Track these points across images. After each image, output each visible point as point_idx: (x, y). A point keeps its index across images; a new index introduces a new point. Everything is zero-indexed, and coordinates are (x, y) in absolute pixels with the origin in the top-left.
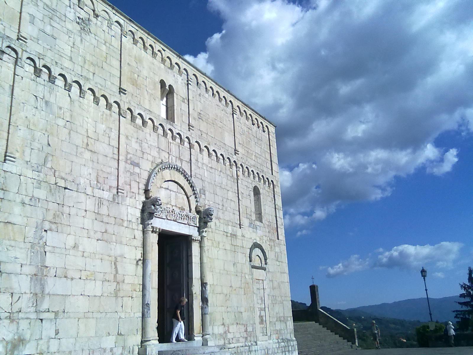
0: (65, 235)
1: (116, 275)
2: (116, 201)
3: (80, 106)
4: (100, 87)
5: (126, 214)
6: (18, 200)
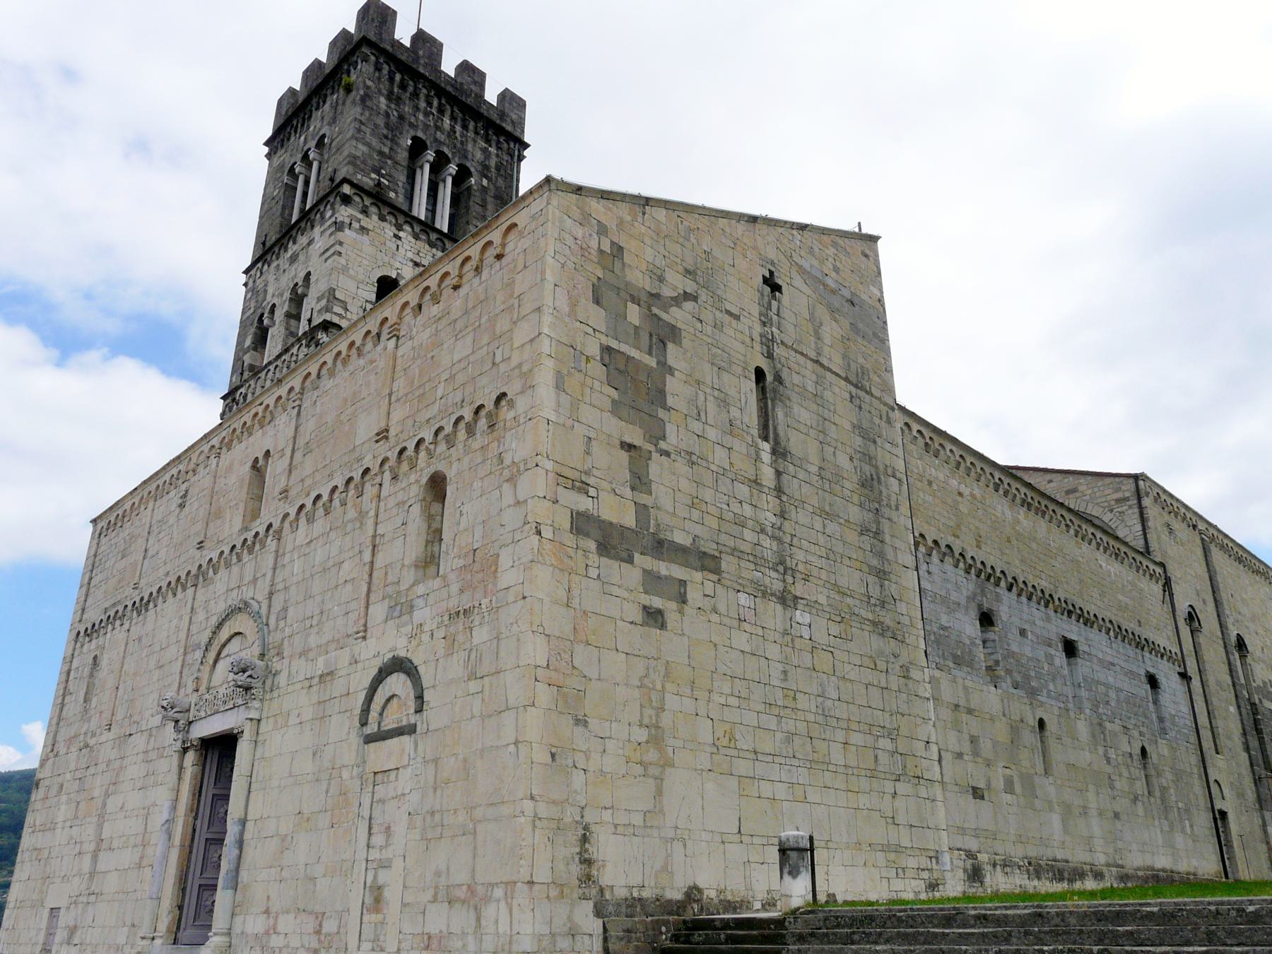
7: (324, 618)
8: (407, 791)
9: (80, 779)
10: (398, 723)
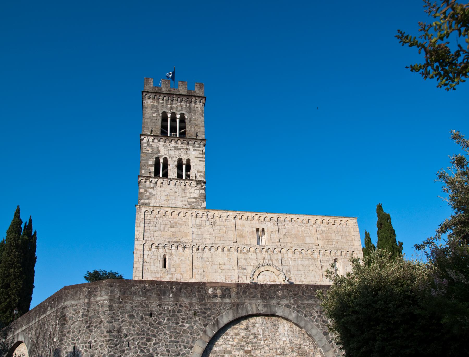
3: (215, 255)
4: (223, 244)
7: (306, 276)
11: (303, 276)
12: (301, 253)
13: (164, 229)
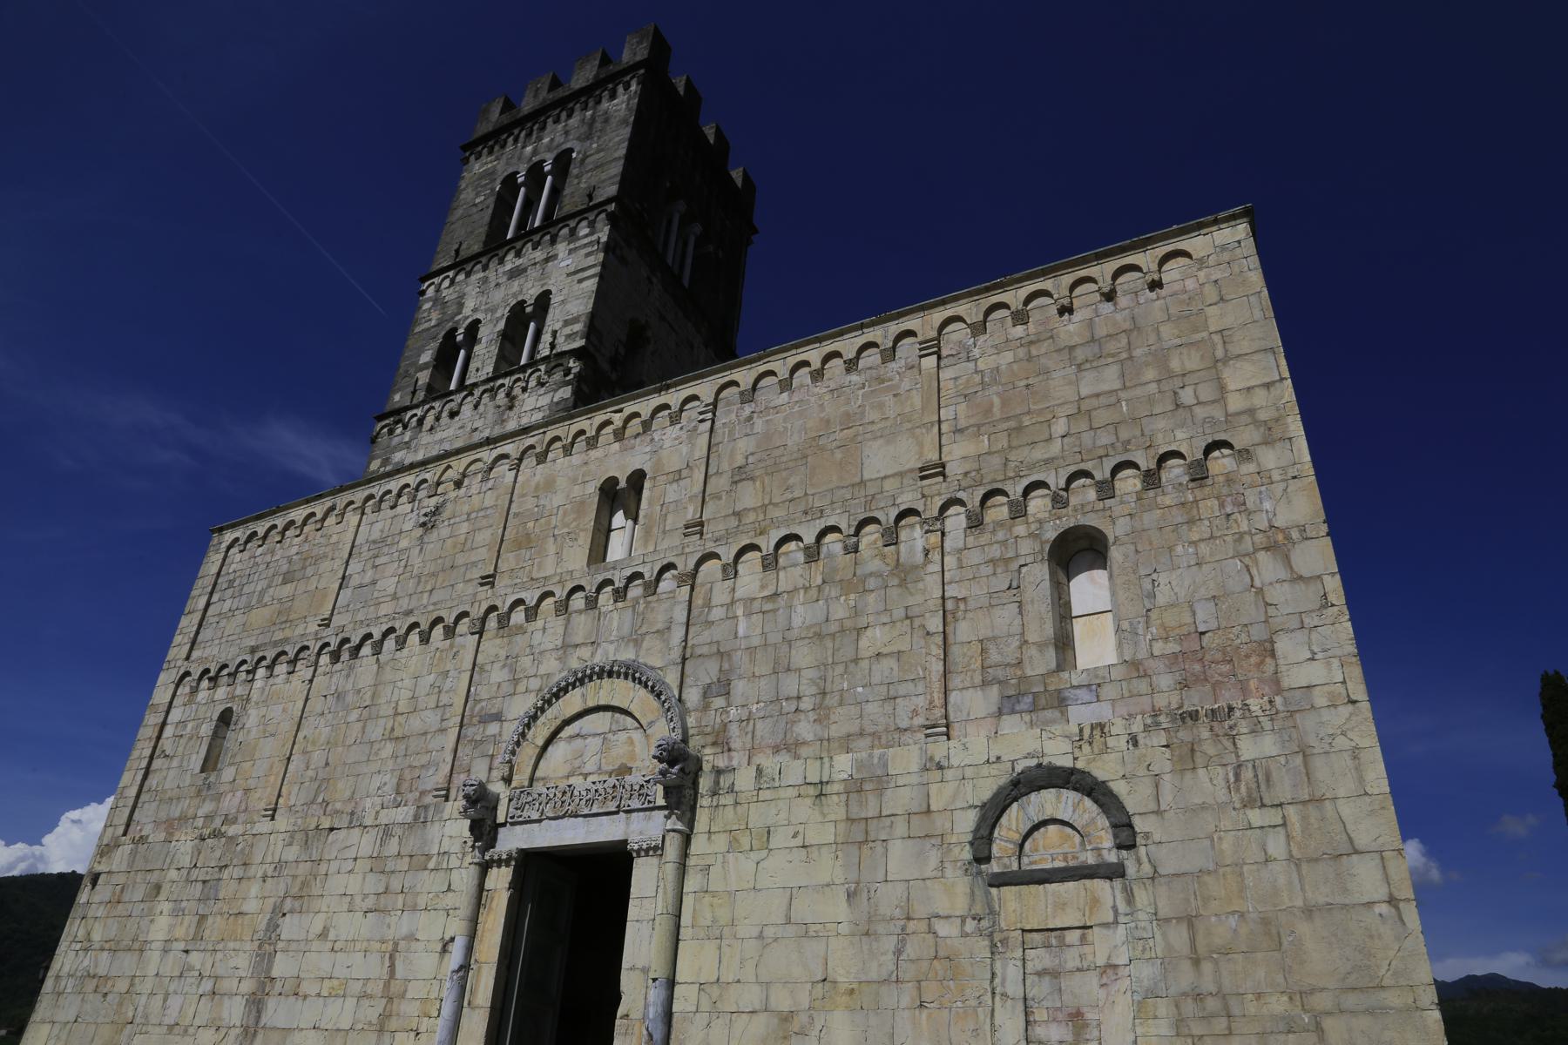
0: (312, 915)
1: (389, 982)
2: (422, 820)
5: (437, 841)
6: (260, 874)
7: (831, 700)
8: (1123, 960)
9: (204, 882)
10: (1065, 859)
11: (806, 704)
12: (812, 554)
13: (263, 592)
